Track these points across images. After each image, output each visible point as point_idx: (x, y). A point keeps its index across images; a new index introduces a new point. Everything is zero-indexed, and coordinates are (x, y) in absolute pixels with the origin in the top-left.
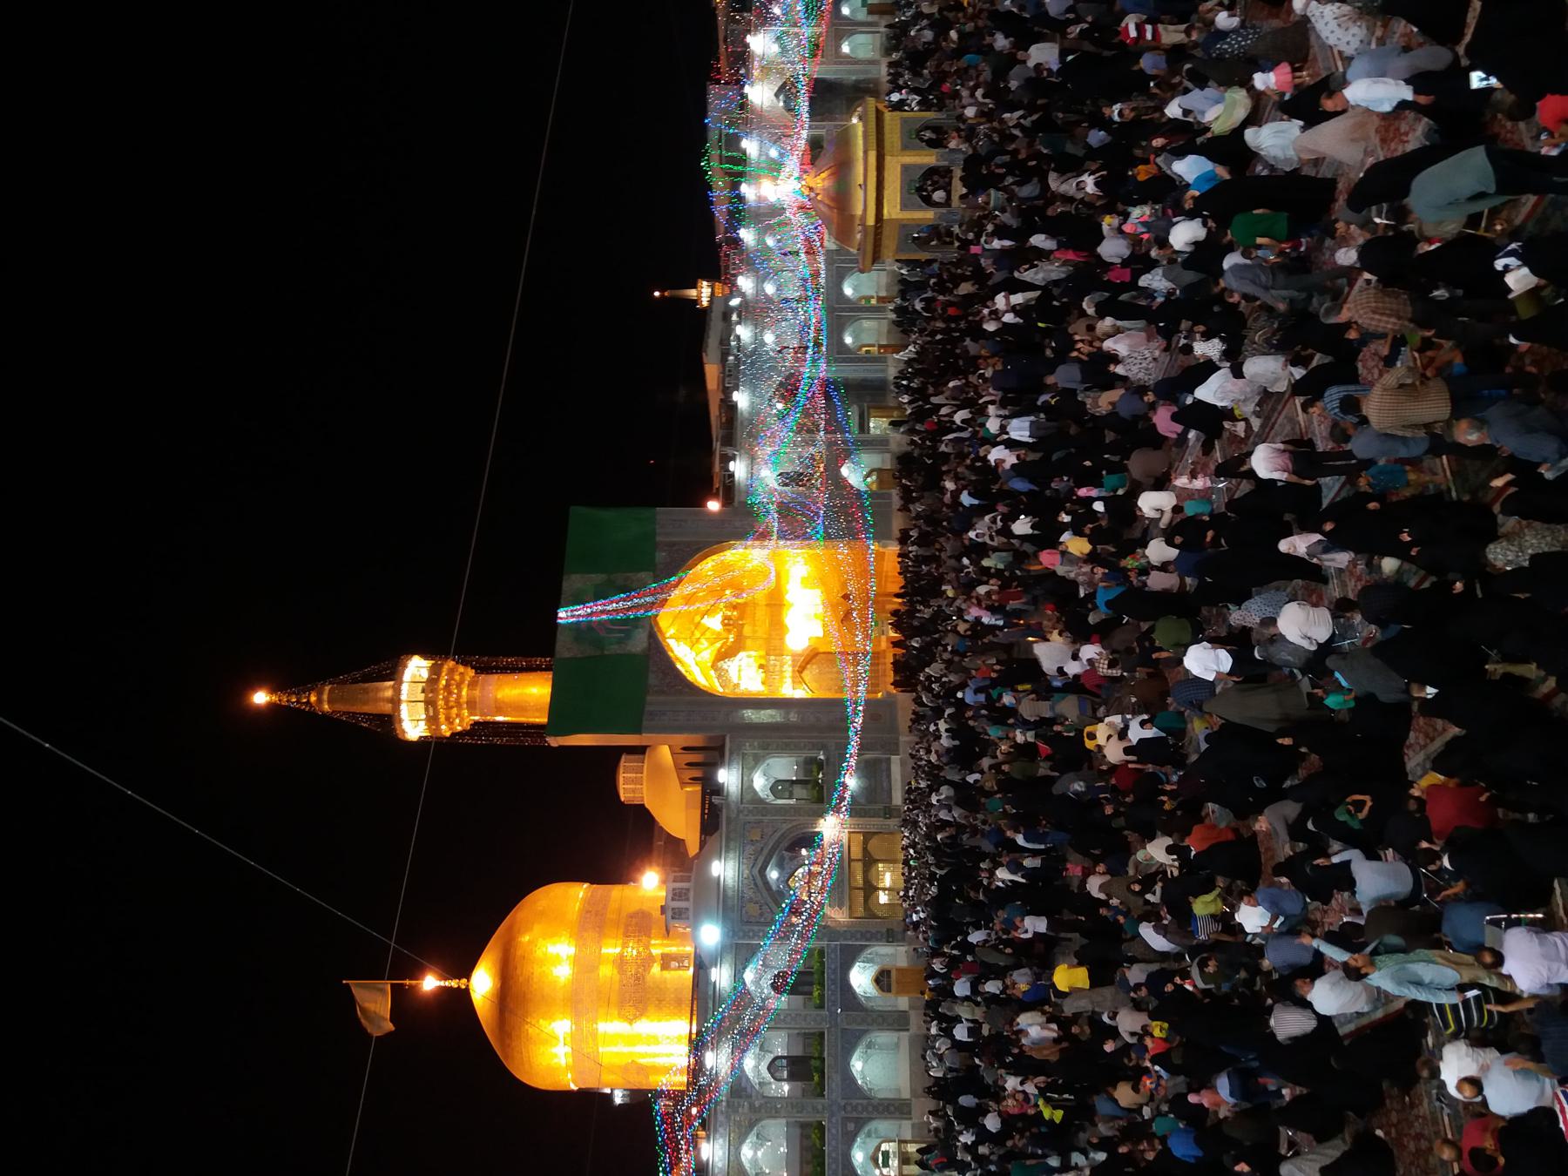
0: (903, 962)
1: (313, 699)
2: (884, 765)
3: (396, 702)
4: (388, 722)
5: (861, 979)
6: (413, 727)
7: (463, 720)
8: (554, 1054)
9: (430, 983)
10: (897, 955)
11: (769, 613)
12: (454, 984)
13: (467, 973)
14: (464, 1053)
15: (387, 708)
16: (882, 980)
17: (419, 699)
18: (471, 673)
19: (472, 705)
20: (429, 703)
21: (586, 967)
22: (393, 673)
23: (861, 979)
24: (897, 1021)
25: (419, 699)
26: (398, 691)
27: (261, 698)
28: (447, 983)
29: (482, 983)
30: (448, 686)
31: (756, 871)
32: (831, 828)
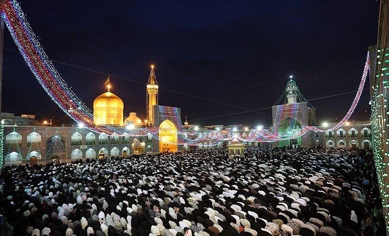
0: (127, 154)
3: (151, 84)
4: (149, 83)
5: (125, 149)
6: (148, 86)
7: (150, 94)
8: (99, 105)
10: (128, 153)
11: (169, 134)
13: (110, 92)
16: (125, 151)
17: (152, 88)
20: (153, 89)
21: (114, 109)
23: (125, 149)
24: (120, 154)
25: (152, 88)
27: (152, 67)
29: (109, 94)
32: (143, 144)
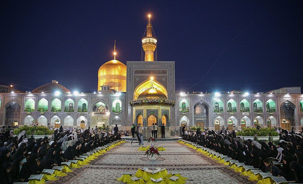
1: (149, 24)
2: (120, 123)
8: (102, 73)
9: (115, 53)
12: (115, 57)
14: (103, 59)
16: (83, 122)
17: (149, 42)
18: (154, 50)
20: (146, 43)
22: (154, 37)
23: (82, 118)
25: (149, 42)
26: (150, 37)
28: (115, 56)
29: (115, 61)
31: (100, 100)
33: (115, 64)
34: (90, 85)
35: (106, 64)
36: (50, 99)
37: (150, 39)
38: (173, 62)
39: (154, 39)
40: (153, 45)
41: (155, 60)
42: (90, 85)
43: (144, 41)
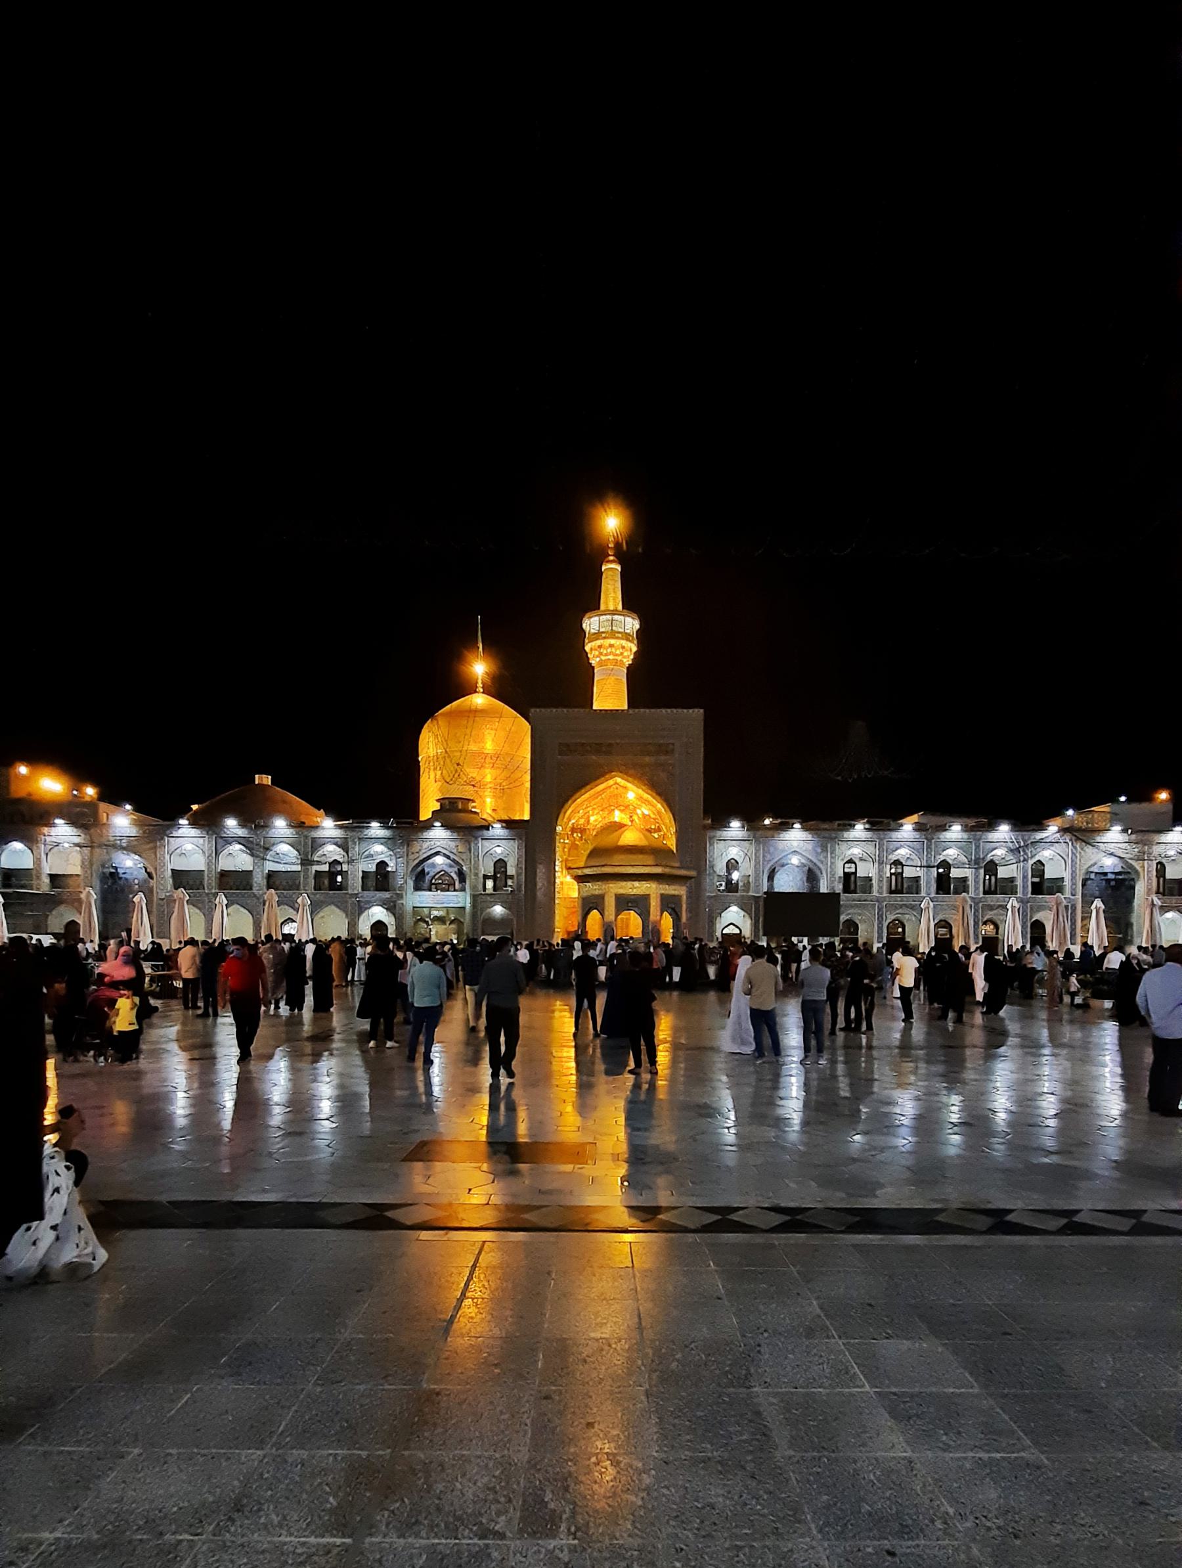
15: (602, 607)
18: (628, 661)
19: (601, 663)
20: (598, 635)
23: (378, 913)
26: (614, 612)
27: (612, 522)
30: (611, 646)
31: (438, 849)
33: (482, 711)
34: (379, 788)
35: (450, 713)
36: (258, 848)
37: (616, 617)
38: (696, 714)
39: (628, 619)
40: (624, 643)
41: (631, 704)
42: (379, 788)
43: (591, 624)
